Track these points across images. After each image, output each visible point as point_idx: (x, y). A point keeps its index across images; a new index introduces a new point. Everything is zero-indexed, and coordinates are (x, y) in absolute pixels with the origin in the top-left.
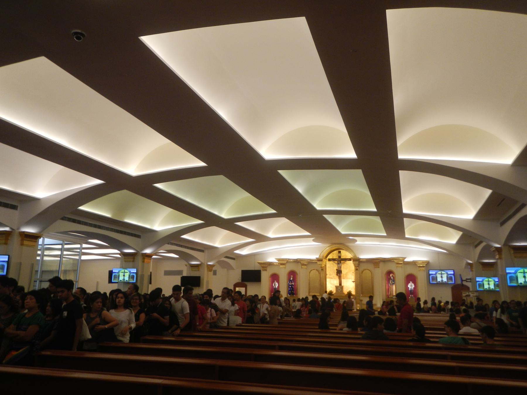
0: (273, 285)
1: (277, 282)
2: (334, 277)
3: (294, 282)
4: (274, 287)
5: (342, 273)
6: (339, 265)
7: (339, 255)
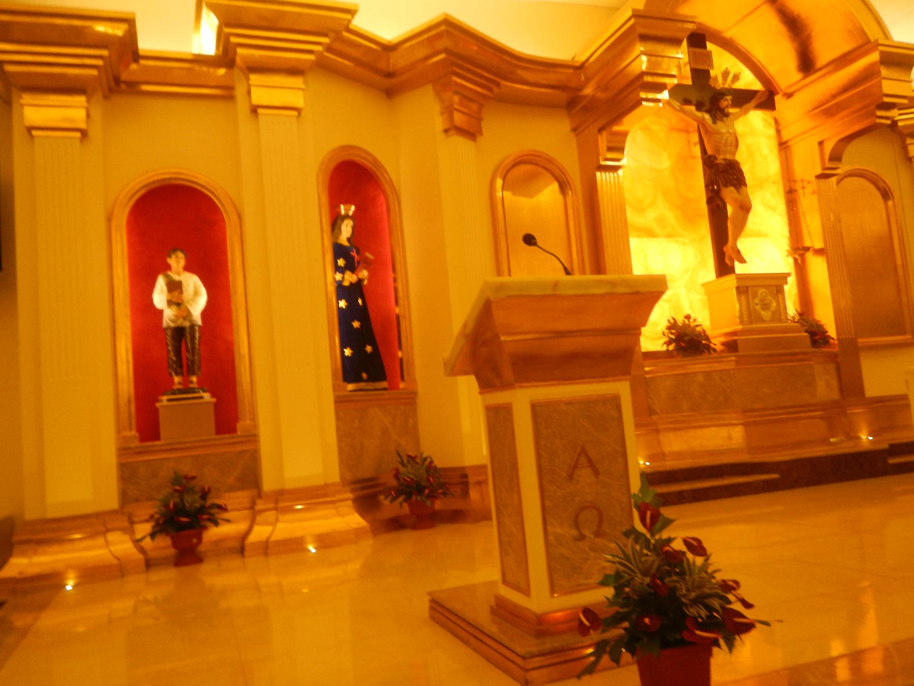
0: (159, 297)
1: (188, 268)
2: (661, 221)
3: (367, 264)
4: (169, 314)
5: (745, 185)
6: (721, 127)
7: (700, 67)
